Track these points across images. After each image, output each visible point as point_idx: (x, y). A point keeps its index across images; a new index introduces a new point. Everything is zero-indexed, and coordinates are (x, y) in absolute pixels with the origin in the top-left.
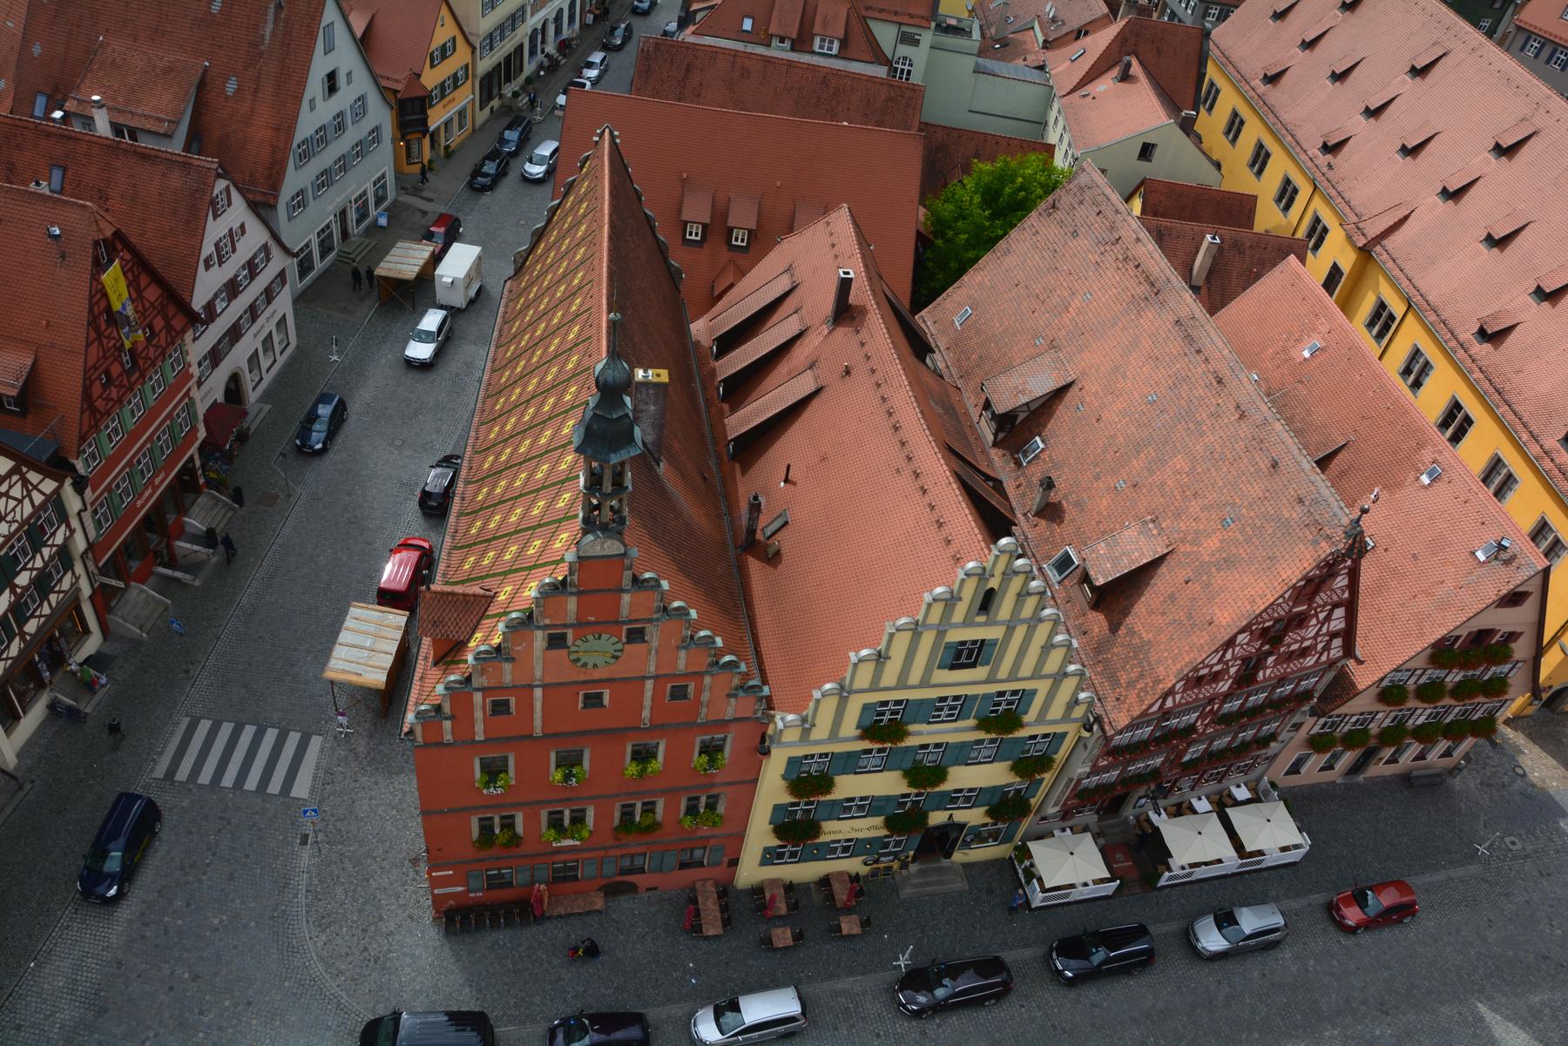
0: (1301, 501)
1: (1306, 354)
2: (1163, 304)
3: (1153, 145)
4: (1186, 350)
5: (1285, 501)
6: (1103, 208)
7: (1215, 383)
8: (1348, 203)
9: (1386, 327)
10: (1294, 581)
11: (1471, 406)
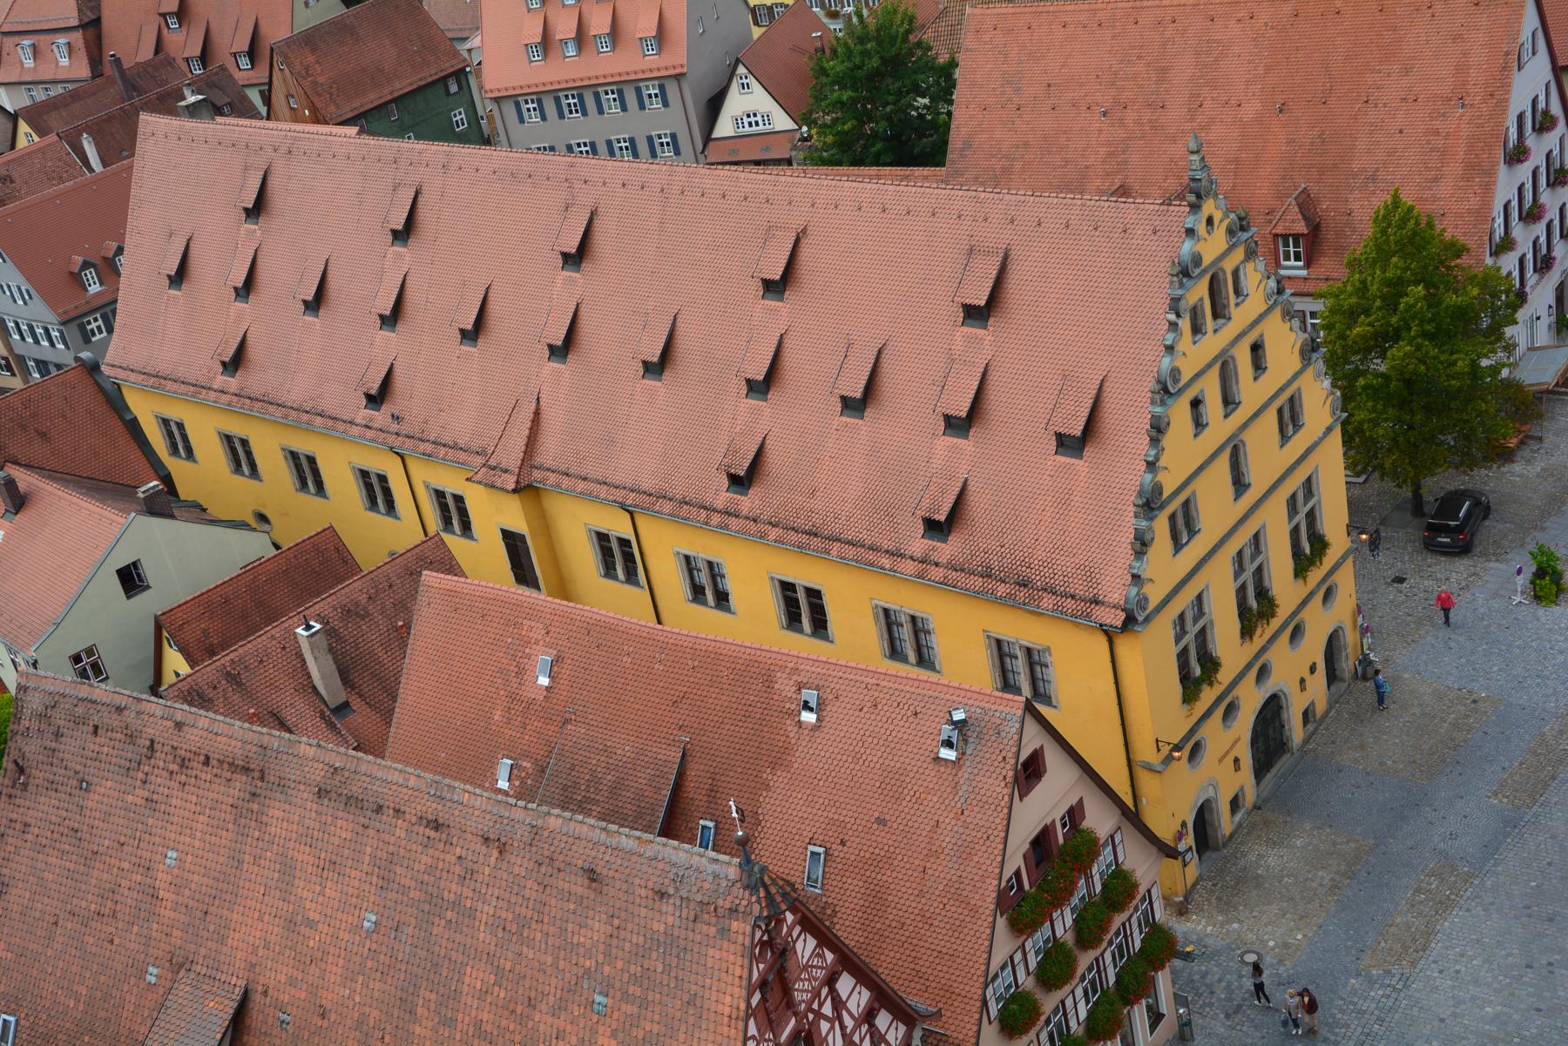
0: (662, 895)
1: (544, 681)
2: (282, 785)
3: (135, 564)
4: (362, 820)
5: (643, 912)
6: (96, 719)
7: (433, 834)
8: (455, 447)
9: (629, 558)
10: (743, 1006)
11: (805, 574)
